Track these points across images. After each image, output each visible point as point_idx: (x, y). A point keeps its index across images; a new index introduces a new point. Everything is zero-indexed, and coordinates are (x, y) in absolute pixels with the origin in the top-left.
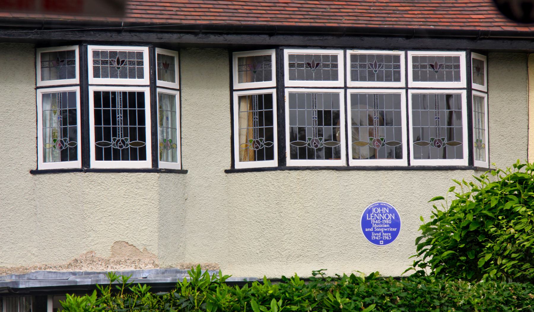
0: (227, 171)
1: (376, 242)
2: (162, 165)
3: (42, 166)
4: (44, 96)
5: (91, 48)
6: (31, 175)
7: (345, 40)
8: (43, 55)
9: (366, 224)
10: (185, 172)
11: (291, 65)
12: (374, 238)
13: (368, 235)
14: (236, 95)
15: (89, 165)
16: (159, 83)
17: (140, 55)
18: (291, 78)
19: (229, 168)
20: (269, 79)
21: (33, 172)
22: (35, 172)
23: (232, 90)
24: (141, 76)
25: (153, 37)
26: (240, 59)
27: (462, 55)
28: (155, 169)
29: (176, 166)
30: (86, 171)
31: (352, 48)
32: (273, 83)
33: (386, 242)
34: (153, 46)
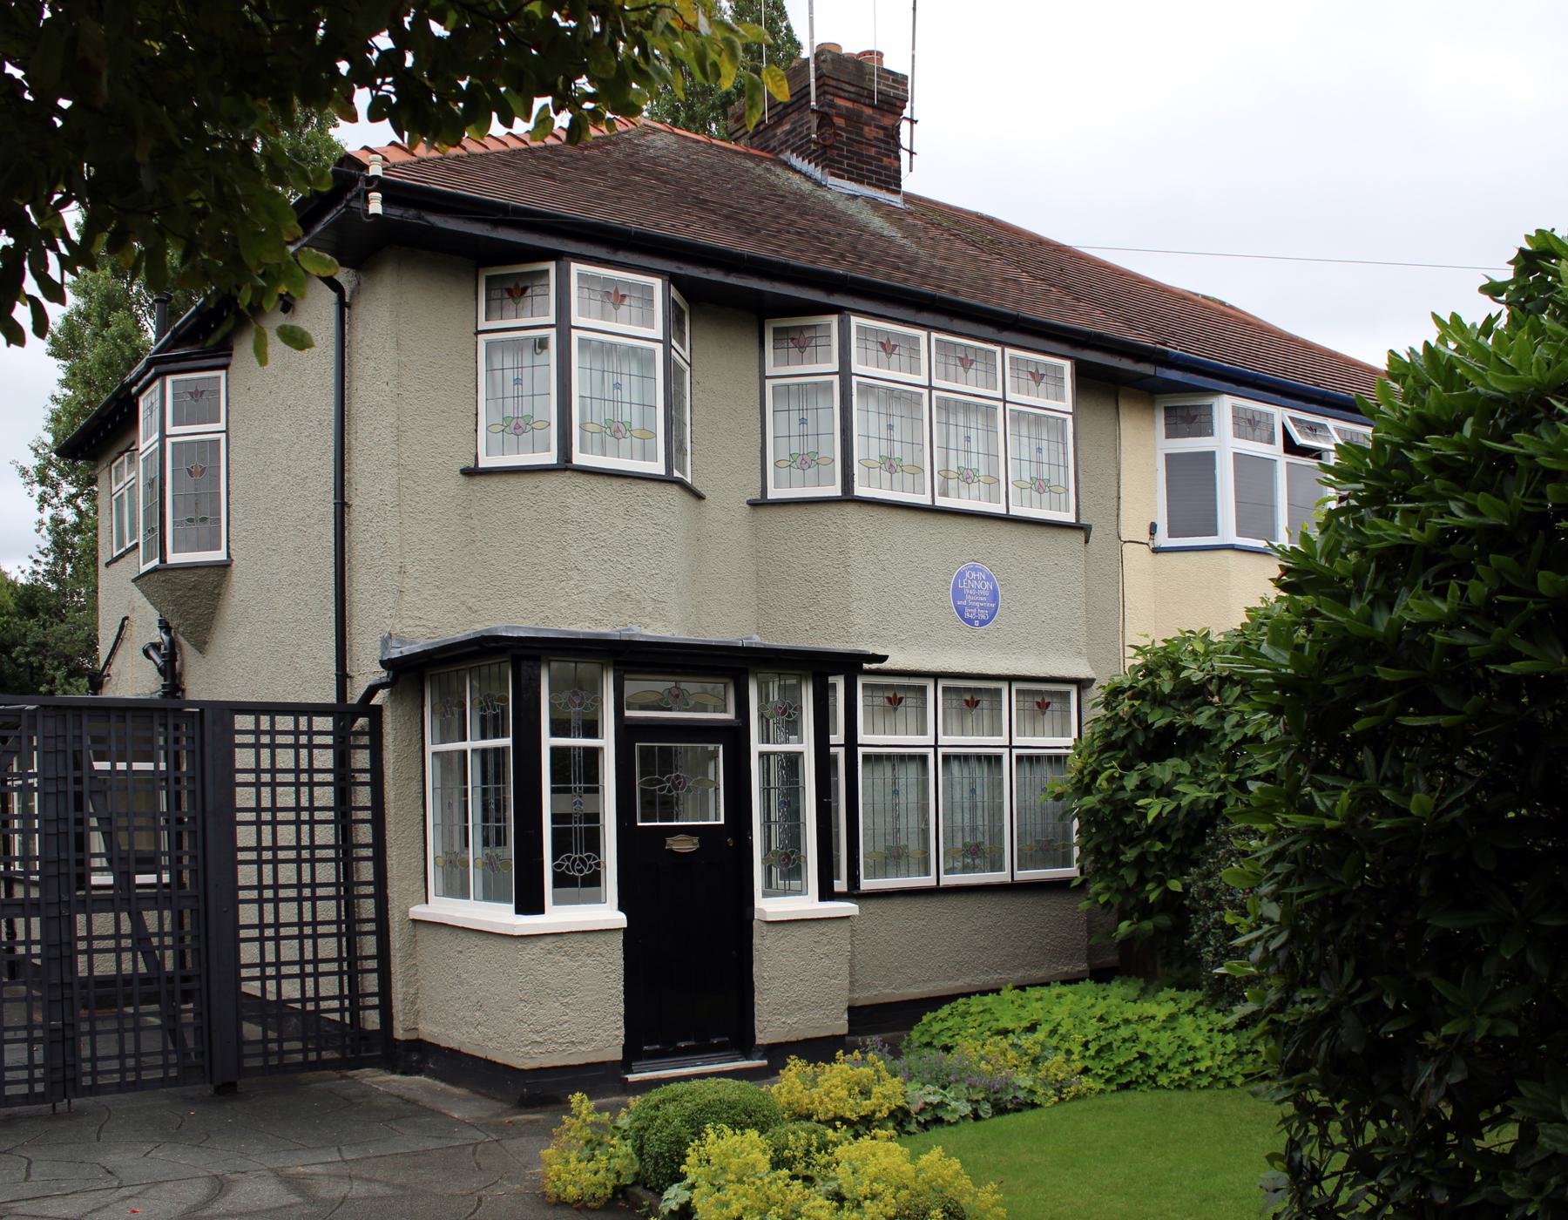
0: (754, 504)
1: (970, 622)
3: (485, 462)
6: (462, 479)
7: (925, 318)
9: (958, 594)
10: (699, 497)
12: (967, 615)
13: (961, 611)
14: (769, 384)
15: (570, 461)
19: (757, 496)
22: (472, 472)
23: (763, 377)
25: (671, 267)
26: (776, 331)
27: (1067, 365)
28: (666, 480)
30: (566, 469)
31: (939, 330)
33: (983, 623)
34: (672, 279)
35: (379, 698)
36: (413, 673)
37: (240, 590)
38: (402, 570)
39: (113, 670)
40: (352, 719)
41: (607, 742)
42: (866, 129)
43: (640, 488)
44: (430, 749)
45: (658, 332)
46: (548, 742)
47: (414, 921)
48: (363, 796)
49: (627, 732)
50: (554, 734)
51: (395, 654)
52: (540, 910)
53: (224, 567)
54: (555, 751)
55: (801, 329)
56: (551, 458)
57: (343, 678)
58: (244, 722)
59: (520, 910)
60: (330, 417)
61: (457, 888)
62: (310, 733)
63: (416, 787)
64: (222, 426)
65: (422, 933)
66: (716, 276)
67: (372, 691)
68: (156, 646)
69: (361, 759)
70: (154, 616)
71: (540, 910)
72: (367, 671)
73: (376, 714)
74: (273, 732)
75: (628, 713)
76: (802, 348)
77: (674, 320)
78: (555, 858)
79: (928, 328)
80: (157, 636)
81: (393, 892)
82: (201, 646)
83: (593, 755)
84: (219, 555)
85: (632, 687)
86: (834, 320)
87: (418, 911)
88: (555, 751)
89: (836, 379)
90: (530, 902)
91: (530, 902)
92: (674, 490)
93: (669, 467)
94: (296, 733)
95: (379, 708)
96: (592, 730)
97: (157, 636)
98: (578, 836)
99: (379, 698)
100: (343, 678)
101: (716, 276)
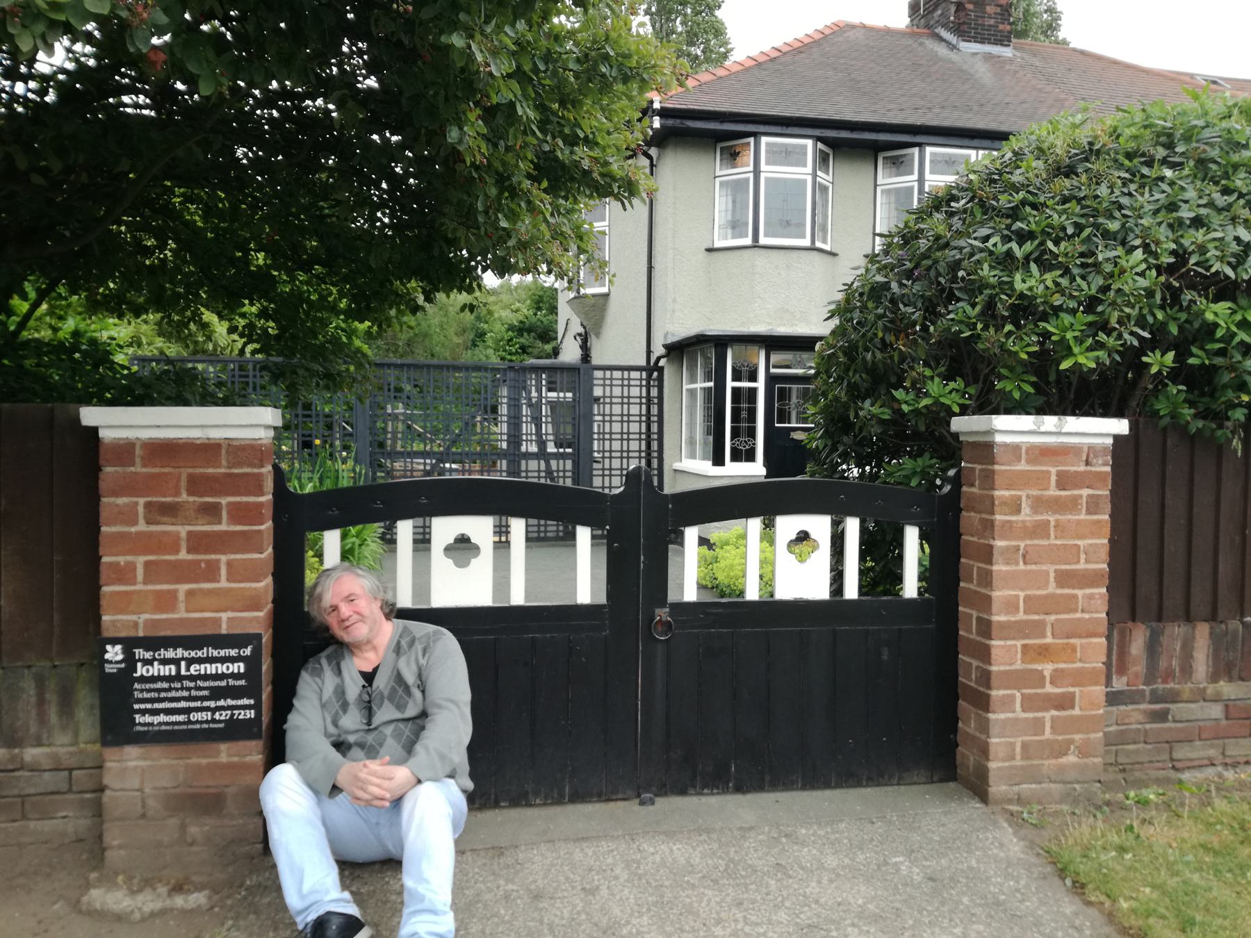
2: (818, 244)
3: (717, 245)
4: (721, 184)
5: (764, 140)
7: (976, 142)
8: (722, 149)
11: (931, 161)
16: (819, 173)
17: (805, 147)
18: (931, 173)
19: (870, 252)
20: (912, 173)
21: (709, 250)
23: (876, 186)
24: (805, 165)
25: (818, 132)
29: (827, 247)
32: (915, 177)
35: (662, 363)
36: (680, 350)
37: (614, 308)
38: (674, 301)
39: (563, 346)
40: (652, 370)
41: (760, 385)
42: (988, 8)
43: (795, 254)
44: (685, 387)
45: (809, 169)
46: (730, 384)
47: (675, 470)
48: (654, 410)
49: (771, 380)
50: (734, 380)
51: (669, 341)
52: (723, 464)
53: (606, 296)
54: (734, 390)
55: (897, 157)
56: (748, 241)
57: (649, 352)
58: (598, 374)
59: (714, 464)
60: (646, 222)
61: (692, 456)
62: (629, 379)
63: (678, 405)
64: (606, 223)
65: (679, 475)
66: (844, 134)
67: (659, 359)
68: (580, 335)
69: (654, 392)
70: (579, 320)
71: (723, 464)
72: (658, 350)
73: (661, 370)
74: (611, 379)
75: (773, 370)
76: (902, 168)
77: (822, 160)
78: (732, 439)
79: (976, 148)
80: (581, 330)
81: (666, 456)
82: (598, 335)
83: (753, 391)
84: (604, 290)
85: (775, 358)
86: (916, 150)
87: (677, 466)
88: (734, 390)
89: (916, 184)
90: (718, 460)
91: (718, 460)
92: (815, 253)
93: (813, 241)
94: (623, 379)
95: (662, 368)
96: (753, 378)
97: (581, 330)
98: (744, 430)
99: (662, 363)
100: (649, 352)
101: (844, 134)
